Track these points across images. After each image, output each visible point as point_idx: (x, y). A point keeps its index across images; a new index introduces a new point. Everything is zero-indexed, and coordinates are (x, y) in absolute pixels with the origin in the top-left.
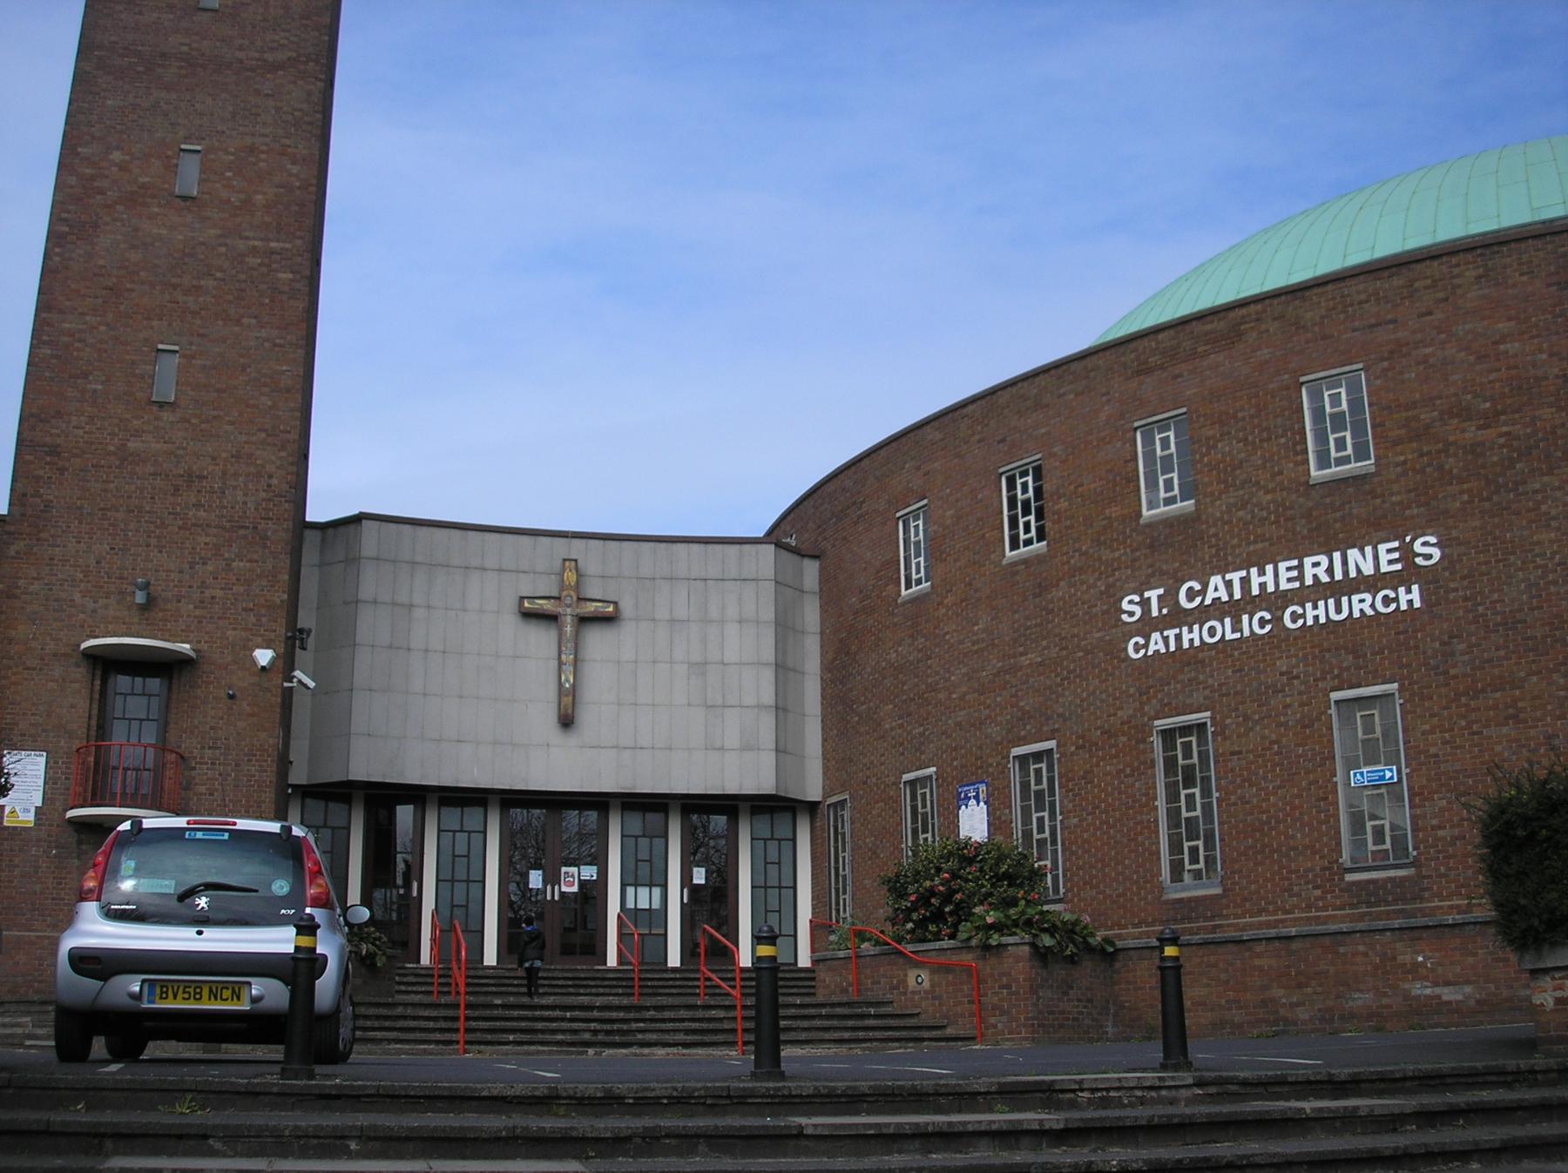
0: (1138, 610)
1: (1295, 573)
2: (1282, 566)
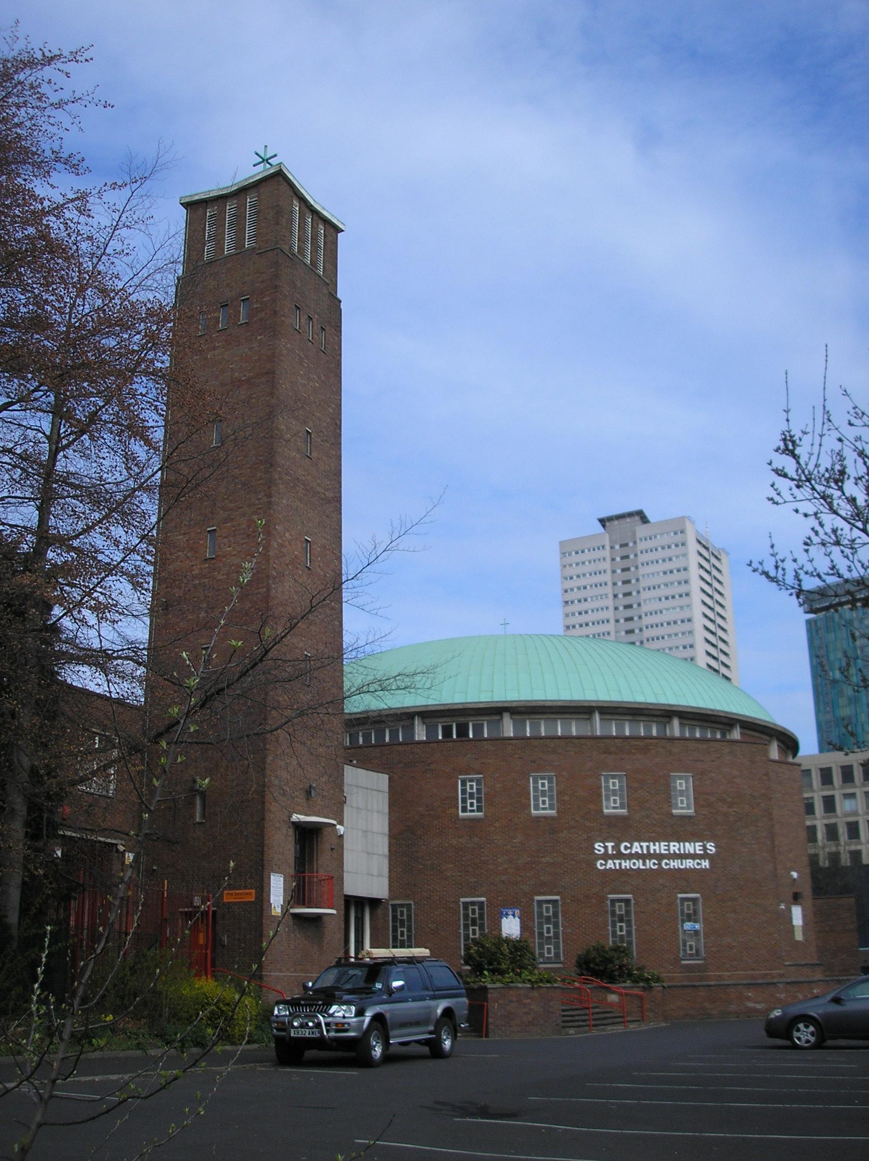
0: (603, 850)
1: (666, 848)
2: (662, 844)
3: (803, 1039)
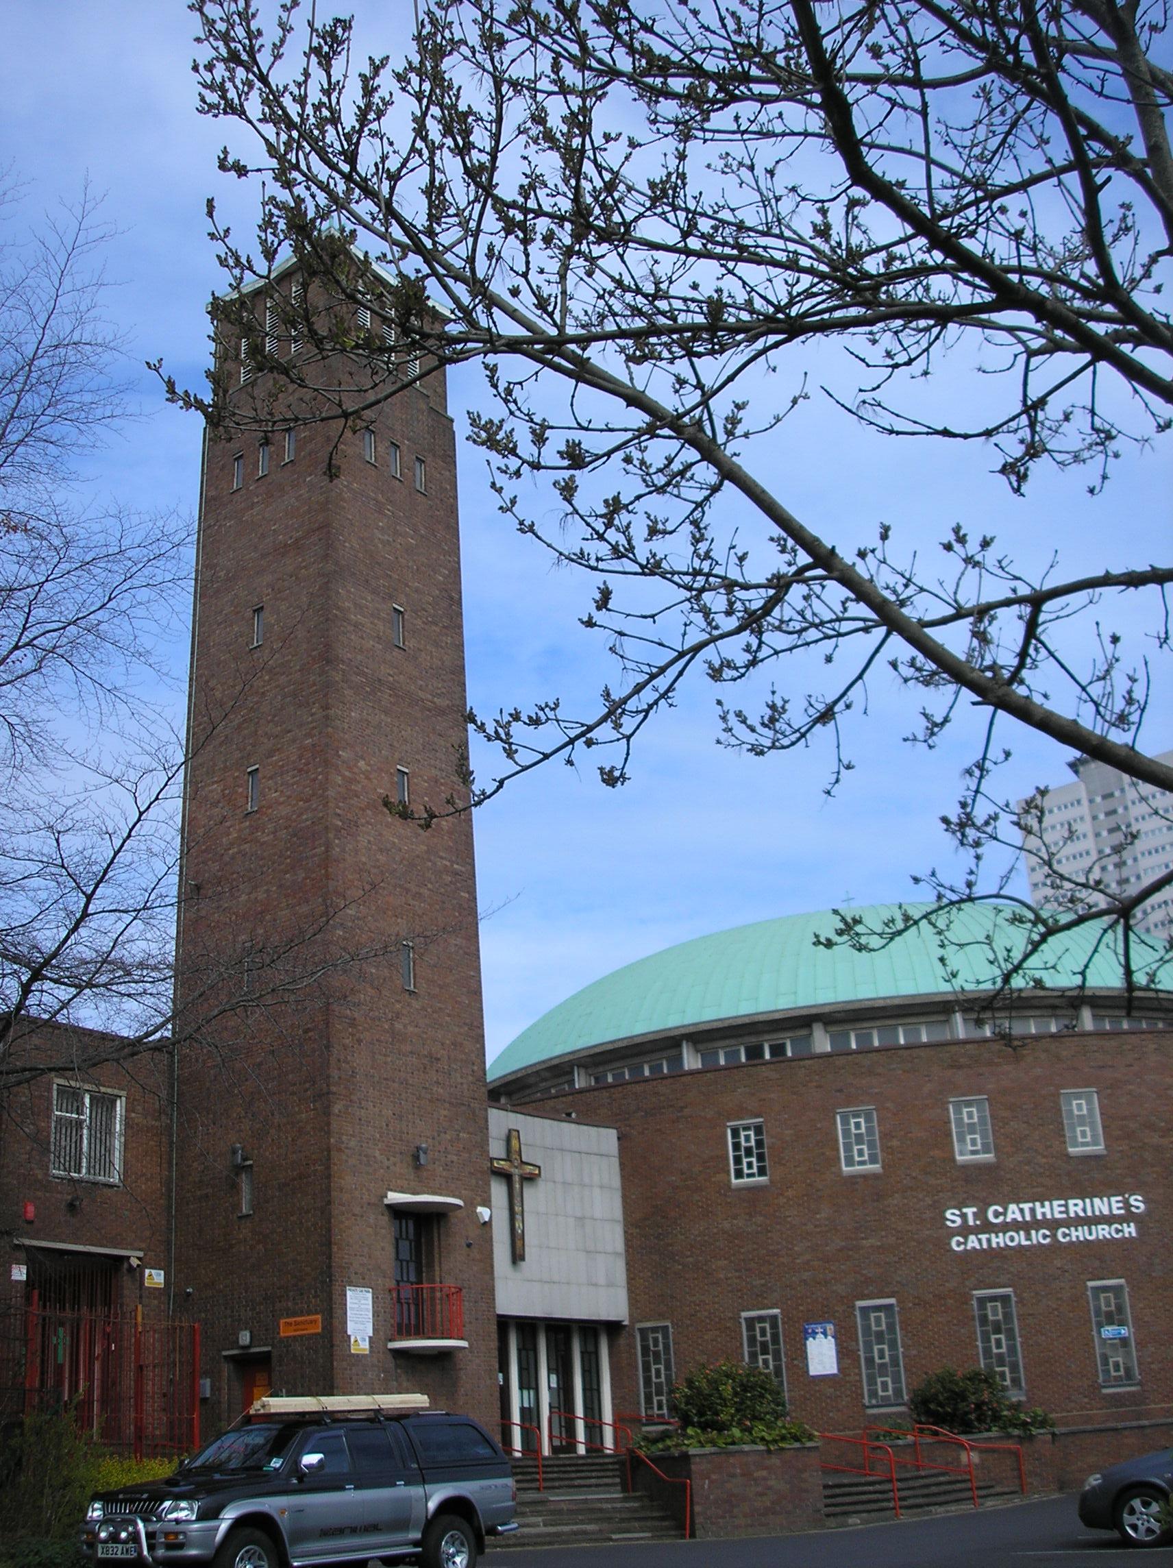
0: (959, 1220)
1: (1063, 1209)
2: (1055, 1203)
3: (1142, 1529)
